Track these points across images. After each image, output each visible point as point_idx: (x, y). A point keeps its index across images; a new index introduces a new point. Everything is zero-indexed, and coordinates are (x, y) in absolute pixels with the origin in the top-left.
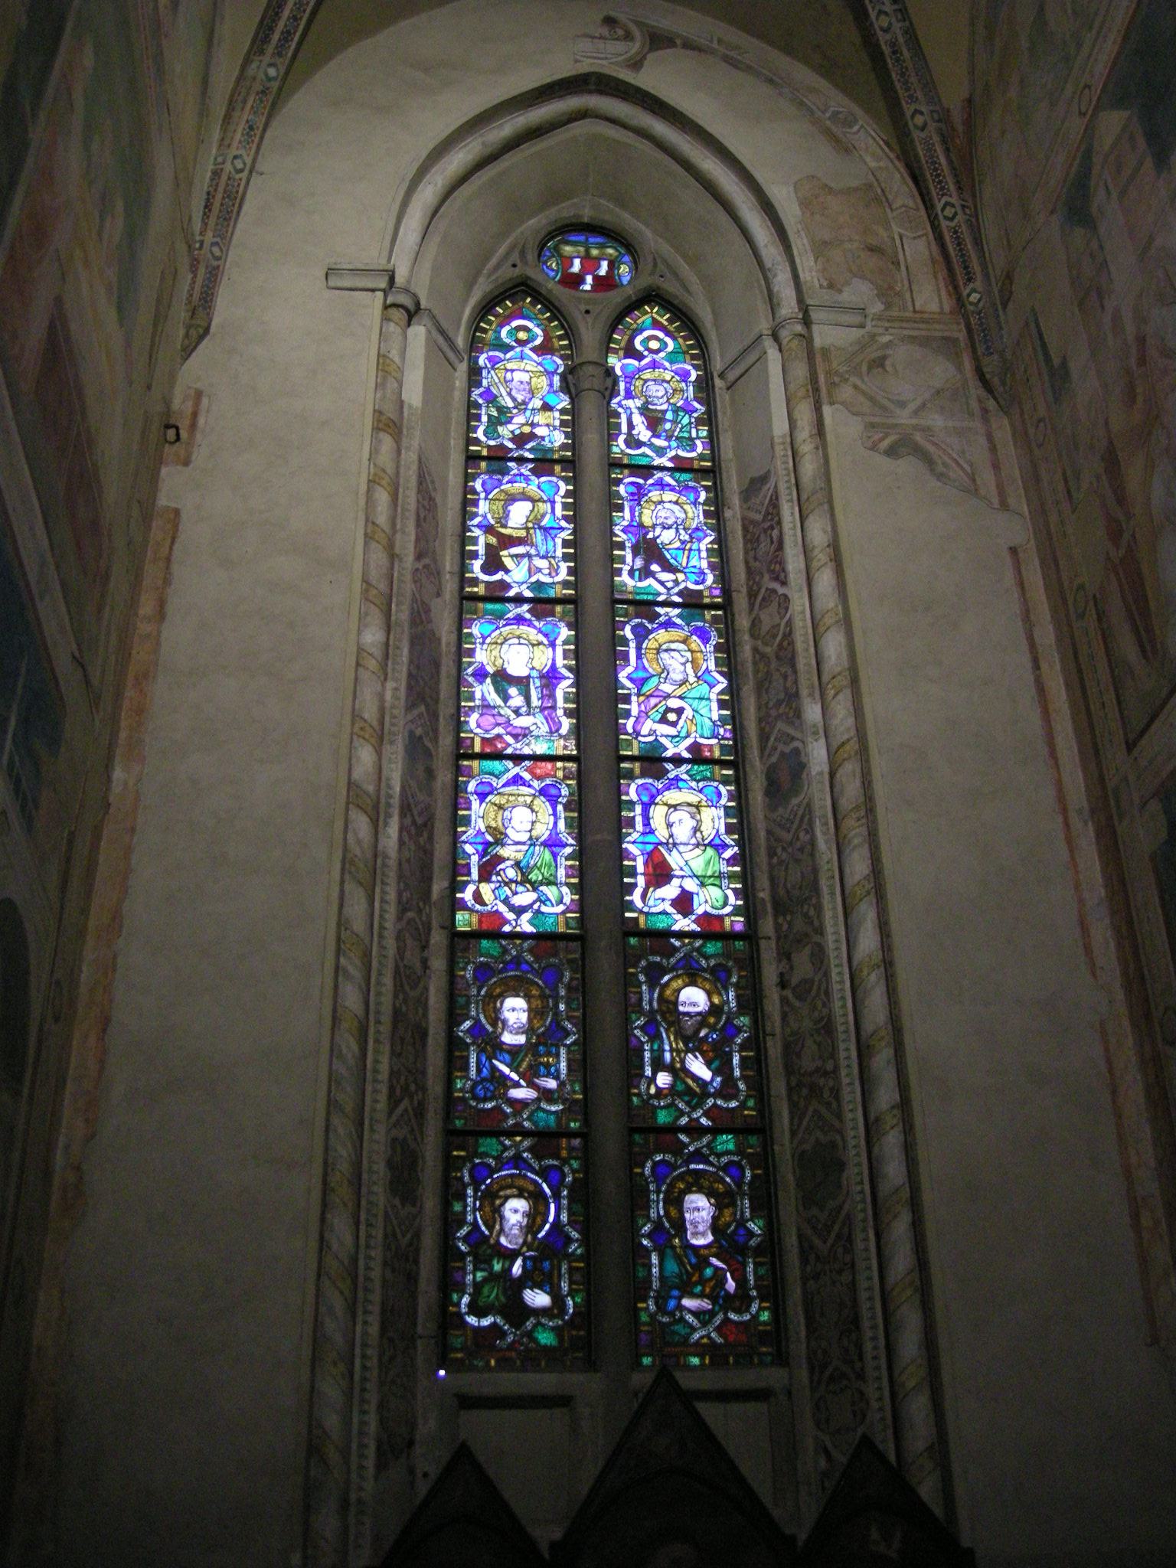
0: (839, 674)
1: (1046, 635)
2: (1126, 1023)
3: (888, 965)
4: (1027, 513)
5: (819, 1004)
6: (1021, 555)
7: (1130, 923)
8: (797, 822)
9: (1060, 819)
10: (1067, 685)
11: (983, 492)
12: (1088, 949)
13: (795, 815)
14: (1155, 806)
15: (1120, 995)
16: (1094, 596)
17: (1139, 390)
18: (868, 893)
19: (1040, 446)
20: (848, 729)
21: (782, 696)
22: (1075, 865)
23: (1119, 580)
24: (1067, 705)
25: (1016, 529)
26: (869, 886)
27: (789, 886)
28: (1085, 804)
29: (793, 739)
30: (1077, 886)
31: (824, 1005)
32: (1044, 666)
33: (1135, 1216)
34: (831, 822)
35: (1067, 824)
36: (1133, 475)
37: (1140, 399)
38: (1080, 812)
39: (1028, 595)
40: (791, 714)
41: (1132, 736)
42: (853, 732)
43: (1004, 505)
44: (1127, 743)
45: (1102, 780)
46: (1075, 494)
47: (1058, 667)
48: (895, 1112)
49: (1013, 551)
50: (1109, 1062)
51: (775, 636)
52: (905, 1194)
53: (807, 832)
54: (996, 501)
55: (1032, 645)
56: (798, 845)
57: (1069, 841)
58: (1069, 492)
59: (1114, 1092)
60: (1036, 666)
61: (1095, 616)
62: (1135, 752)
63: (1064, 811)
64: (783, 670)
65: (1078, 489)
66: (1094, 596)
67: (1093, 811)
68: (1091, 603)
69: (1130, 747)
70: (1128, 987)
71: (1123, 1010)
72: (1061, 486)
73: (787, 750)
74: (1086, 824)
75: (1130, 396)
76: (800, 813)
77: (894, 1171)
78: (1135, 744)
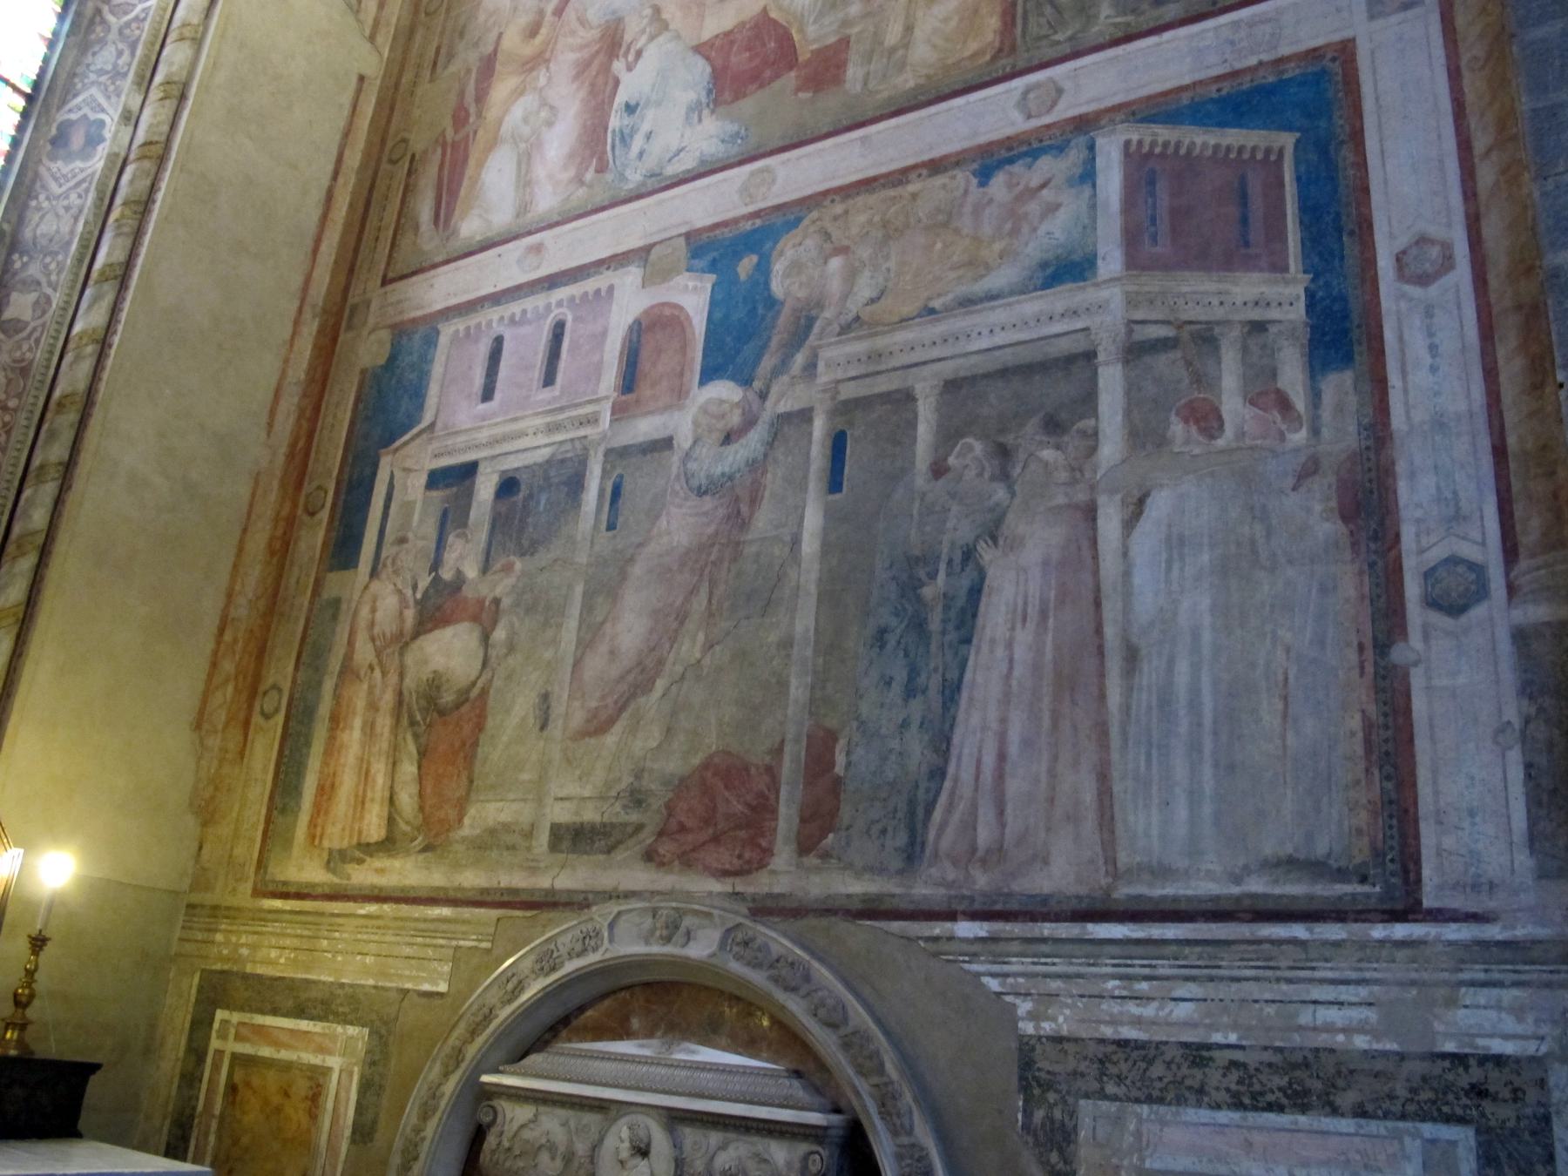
0: (175, 83)
1: (354, 159)
2: (275, 484)
3: (104, 344)
4: (386, 54)
5: (25, 347)
6: (365, 85)
7: (317, 409)
8: (72, 183)
9: (296, 304)
10: (351, 205)
11: (362, 16)
12: (272, 413)
13: (74, 176)
14: (385, 335)
15: (281, 459)
16: (413, 156)
17: (543, 31)
18: (115, 278)
19: (427, 14)
20: (161, 134)
21: (109, 67)
22: (292, 346)
23: (444, 154)
24: (342, 221)
25: (370, 62)
26: (119, 272)
27: (38, 232)
28: (321, 304)
29: (103, 110)
30: (286, 361)
31: (30, 349)
32: (341, 180)
33: (221, 631)
34: (107, 201)
35: (300, 311)
36: (500, 90)
37: (539, 39)
38: (314, 306)
39: (355, 119)
40: (111, 88)
41: (391, 275)
42: (163, 138)
43: (372, 38)
44: (384, 277)
45: (346, 290)
46: (439, 70)
47: (350, 188)
48: (61, 468)
49: (361, 78)
50: (251, 505)
51: (126, 13)
52: (40, 539)
53: (80, 196)
54: (367, 32)
55: (339, 160)
56: (65, 203)
57: (297, 323)
58: (435, 63)
59: (245, 530)
60: (335, 176)
61: (405, 171)
62: (389, 288)
63: (303, 300)
64: (121, 46)
65: (445, 67)
66: (413, 156)
67: (325, 311)
68: (408, 158)
69: (385, 282)
70: (291, 456)
71: (278, 473)
72: (431, 53)
73: (92, 116)
74: (314, 317)
75: (533, 31)
76: (80, 177)
77: (38, 518)
78: (393, 280)
